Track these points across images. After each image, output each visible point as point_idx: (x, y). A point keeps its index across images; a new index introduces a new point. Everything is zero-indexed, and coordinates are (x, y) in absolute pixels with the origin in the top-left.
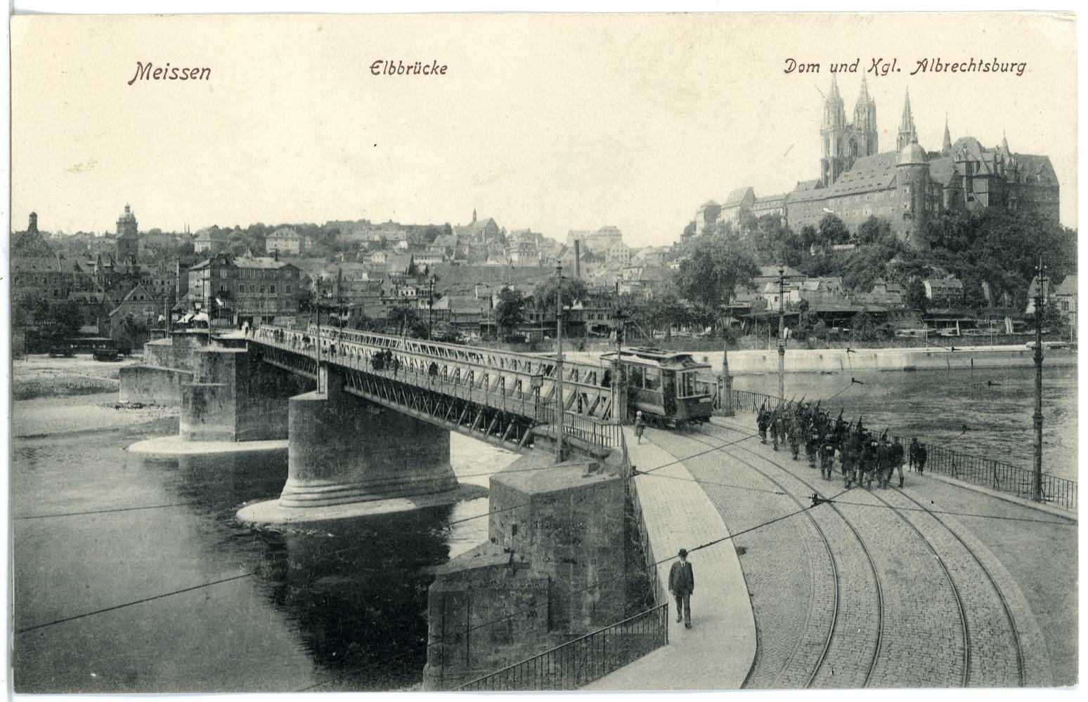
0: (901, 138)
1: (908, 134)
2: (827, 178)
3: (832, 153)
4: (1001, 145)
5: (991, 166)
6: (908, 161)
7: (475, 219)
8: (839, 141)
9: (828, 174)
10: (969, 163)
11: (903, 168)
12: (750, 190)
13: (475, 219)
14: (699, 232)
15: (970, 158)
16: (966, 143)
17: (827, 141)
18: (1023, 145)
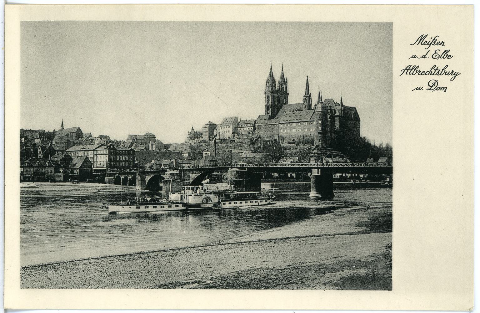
0: (305, 98)
1: (308, 97)
2: (268, 113)
3: (270, 103)
4: (340, 102)
5: (340, 111)
6: (321, 111)
7: (63, 127)
8: (273, 97)
9: (269, 111)
10: (331, 110)
11: (318, 113)
12: (236, 118)
13: (63, 127)
14: (206, 137)
15: (332, 109)
16: (329, 101)
17: (268, 97)
18: (348, 103)
